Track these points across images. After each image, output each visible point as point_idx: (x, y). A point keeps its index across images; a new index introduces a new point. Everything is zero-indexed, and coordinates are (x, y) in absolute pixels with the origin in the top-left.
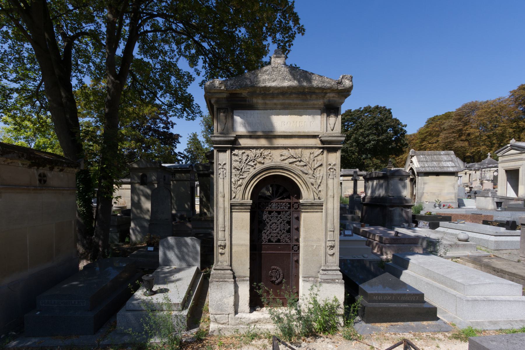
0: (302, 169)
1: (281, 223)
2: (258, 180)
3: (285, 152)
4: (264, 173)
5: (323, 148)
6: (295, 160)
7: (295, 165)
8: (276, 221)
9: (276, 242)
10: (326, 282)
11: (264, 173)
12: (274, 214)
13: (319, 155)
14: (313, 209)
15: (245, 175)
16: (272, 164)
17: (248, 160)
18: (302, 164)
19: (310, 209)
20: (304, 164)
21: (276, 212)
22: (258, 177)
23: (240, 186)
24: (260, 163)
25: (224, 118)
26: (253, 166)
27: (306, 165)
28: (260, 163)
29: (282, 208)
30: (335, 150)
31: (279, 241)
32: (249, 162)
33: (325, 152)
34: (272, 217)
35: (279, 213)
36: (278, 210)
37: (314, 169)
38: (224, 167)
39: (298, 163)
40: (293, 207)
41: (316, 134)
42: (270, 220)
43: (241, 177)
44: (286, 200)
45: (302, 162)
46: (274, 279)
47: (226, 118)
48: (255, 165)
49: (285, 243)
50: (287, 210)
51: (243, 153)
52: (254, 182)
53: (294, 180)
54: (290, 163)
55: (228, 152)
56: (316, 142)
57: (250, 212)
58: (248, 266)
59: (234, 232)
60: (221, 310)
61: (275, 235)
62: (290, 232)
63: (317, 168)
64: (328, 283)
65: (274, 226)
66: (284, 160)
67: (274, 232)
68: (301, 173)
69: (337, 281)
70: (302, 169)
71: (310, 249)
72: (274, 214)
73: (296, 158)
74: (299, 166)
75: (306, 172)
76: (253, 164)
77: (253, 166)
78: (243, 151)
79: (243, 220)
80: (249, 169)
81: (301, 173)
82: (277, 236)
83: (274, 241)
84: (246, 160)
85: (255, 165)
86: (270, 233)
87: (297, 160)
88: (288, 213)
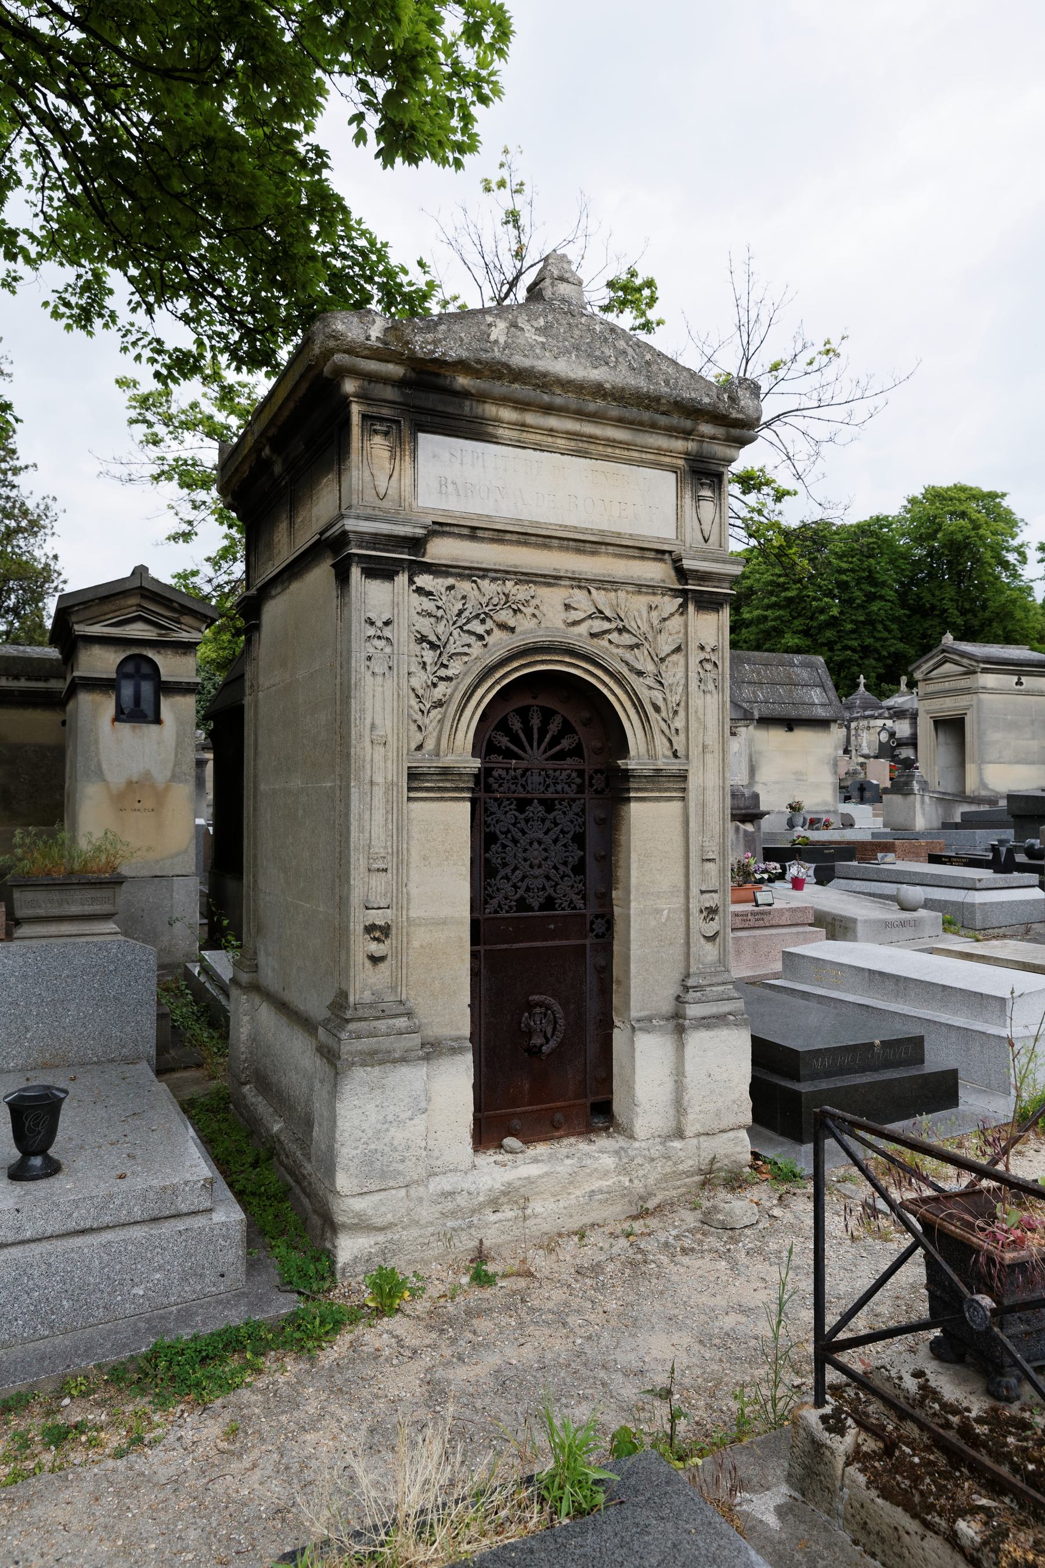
0: (628, 656)
1: (555, 841)
2: (498, 687)
3: (579, 597)
4: (515, 664)
5: (684, 593)
6: (607, 626)
7: (605, 643)
8: (540, 835)
9: (542, 908)
10: (704, 1026)
11: (515, 664)
12: (536, 810)
13: (672, 615)
14: (660, 790)
15: (455, 668)
16: (541, 637)
17: (466, 614)
18: (626, 639)
19: (652, 791)
20: (635, 640)
21: (542, 802)
22: (498, 675)
23: (439, 704)
24: (503, 626)
25: (387, 454)
26: (481, 638)
27: (637, 646)
28: (503, 626)
29: (559, 787)
30: (708, 603)
31: (549, 904)
32: (468, 621)
33: (691, 608)
34: (527, 821)
35: (549, 805)
36: (549, 796)
37: (662, 660)
38: (387, 632)
39: (614, 636)
40: (591, 785)
41: (666, 547)
42: (524, 833)
43: (443, 672)
44: (569, 761)
45: (626, 635)
46: (537, 1040)
47: (393, 457)
48: (489, 632)
49: (568, 912)
50: (572, 795)
51: (450, 588)
52: (485, 694)
53: (605, 691)
54: (593, 635)
55: (402, 579)
56: (657, 572)
57: (474, 802)
58: (465, 997)
59: (421, 873)
60: (383, 1175)
61: (540, 882)
62: (584, 873)
63: (668, 655)
64: (708, 1027)
65: (536, 853)
66: (575, 623)
67: (537, 872)
68: (625, 671)
69: (731, 1018)
70: (628, 656)
71: (653, 923)
72: (536, 810)
73: (609, 620)
74: (618, 646)
75: (639, 667)
76: (480, 629)
77: (481, 638)
78: (451, 581)
79: (446, 827)
80: (469, 645)
81: (625, 671)
82: (544, 888)
83: (536, 904)
84: (459, 615)
85: (489, 632)
86: (524, 878)
87: (613, 626)
88: (576, 808)
